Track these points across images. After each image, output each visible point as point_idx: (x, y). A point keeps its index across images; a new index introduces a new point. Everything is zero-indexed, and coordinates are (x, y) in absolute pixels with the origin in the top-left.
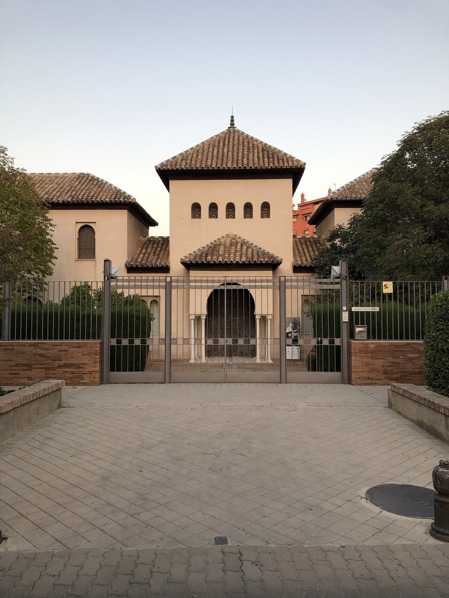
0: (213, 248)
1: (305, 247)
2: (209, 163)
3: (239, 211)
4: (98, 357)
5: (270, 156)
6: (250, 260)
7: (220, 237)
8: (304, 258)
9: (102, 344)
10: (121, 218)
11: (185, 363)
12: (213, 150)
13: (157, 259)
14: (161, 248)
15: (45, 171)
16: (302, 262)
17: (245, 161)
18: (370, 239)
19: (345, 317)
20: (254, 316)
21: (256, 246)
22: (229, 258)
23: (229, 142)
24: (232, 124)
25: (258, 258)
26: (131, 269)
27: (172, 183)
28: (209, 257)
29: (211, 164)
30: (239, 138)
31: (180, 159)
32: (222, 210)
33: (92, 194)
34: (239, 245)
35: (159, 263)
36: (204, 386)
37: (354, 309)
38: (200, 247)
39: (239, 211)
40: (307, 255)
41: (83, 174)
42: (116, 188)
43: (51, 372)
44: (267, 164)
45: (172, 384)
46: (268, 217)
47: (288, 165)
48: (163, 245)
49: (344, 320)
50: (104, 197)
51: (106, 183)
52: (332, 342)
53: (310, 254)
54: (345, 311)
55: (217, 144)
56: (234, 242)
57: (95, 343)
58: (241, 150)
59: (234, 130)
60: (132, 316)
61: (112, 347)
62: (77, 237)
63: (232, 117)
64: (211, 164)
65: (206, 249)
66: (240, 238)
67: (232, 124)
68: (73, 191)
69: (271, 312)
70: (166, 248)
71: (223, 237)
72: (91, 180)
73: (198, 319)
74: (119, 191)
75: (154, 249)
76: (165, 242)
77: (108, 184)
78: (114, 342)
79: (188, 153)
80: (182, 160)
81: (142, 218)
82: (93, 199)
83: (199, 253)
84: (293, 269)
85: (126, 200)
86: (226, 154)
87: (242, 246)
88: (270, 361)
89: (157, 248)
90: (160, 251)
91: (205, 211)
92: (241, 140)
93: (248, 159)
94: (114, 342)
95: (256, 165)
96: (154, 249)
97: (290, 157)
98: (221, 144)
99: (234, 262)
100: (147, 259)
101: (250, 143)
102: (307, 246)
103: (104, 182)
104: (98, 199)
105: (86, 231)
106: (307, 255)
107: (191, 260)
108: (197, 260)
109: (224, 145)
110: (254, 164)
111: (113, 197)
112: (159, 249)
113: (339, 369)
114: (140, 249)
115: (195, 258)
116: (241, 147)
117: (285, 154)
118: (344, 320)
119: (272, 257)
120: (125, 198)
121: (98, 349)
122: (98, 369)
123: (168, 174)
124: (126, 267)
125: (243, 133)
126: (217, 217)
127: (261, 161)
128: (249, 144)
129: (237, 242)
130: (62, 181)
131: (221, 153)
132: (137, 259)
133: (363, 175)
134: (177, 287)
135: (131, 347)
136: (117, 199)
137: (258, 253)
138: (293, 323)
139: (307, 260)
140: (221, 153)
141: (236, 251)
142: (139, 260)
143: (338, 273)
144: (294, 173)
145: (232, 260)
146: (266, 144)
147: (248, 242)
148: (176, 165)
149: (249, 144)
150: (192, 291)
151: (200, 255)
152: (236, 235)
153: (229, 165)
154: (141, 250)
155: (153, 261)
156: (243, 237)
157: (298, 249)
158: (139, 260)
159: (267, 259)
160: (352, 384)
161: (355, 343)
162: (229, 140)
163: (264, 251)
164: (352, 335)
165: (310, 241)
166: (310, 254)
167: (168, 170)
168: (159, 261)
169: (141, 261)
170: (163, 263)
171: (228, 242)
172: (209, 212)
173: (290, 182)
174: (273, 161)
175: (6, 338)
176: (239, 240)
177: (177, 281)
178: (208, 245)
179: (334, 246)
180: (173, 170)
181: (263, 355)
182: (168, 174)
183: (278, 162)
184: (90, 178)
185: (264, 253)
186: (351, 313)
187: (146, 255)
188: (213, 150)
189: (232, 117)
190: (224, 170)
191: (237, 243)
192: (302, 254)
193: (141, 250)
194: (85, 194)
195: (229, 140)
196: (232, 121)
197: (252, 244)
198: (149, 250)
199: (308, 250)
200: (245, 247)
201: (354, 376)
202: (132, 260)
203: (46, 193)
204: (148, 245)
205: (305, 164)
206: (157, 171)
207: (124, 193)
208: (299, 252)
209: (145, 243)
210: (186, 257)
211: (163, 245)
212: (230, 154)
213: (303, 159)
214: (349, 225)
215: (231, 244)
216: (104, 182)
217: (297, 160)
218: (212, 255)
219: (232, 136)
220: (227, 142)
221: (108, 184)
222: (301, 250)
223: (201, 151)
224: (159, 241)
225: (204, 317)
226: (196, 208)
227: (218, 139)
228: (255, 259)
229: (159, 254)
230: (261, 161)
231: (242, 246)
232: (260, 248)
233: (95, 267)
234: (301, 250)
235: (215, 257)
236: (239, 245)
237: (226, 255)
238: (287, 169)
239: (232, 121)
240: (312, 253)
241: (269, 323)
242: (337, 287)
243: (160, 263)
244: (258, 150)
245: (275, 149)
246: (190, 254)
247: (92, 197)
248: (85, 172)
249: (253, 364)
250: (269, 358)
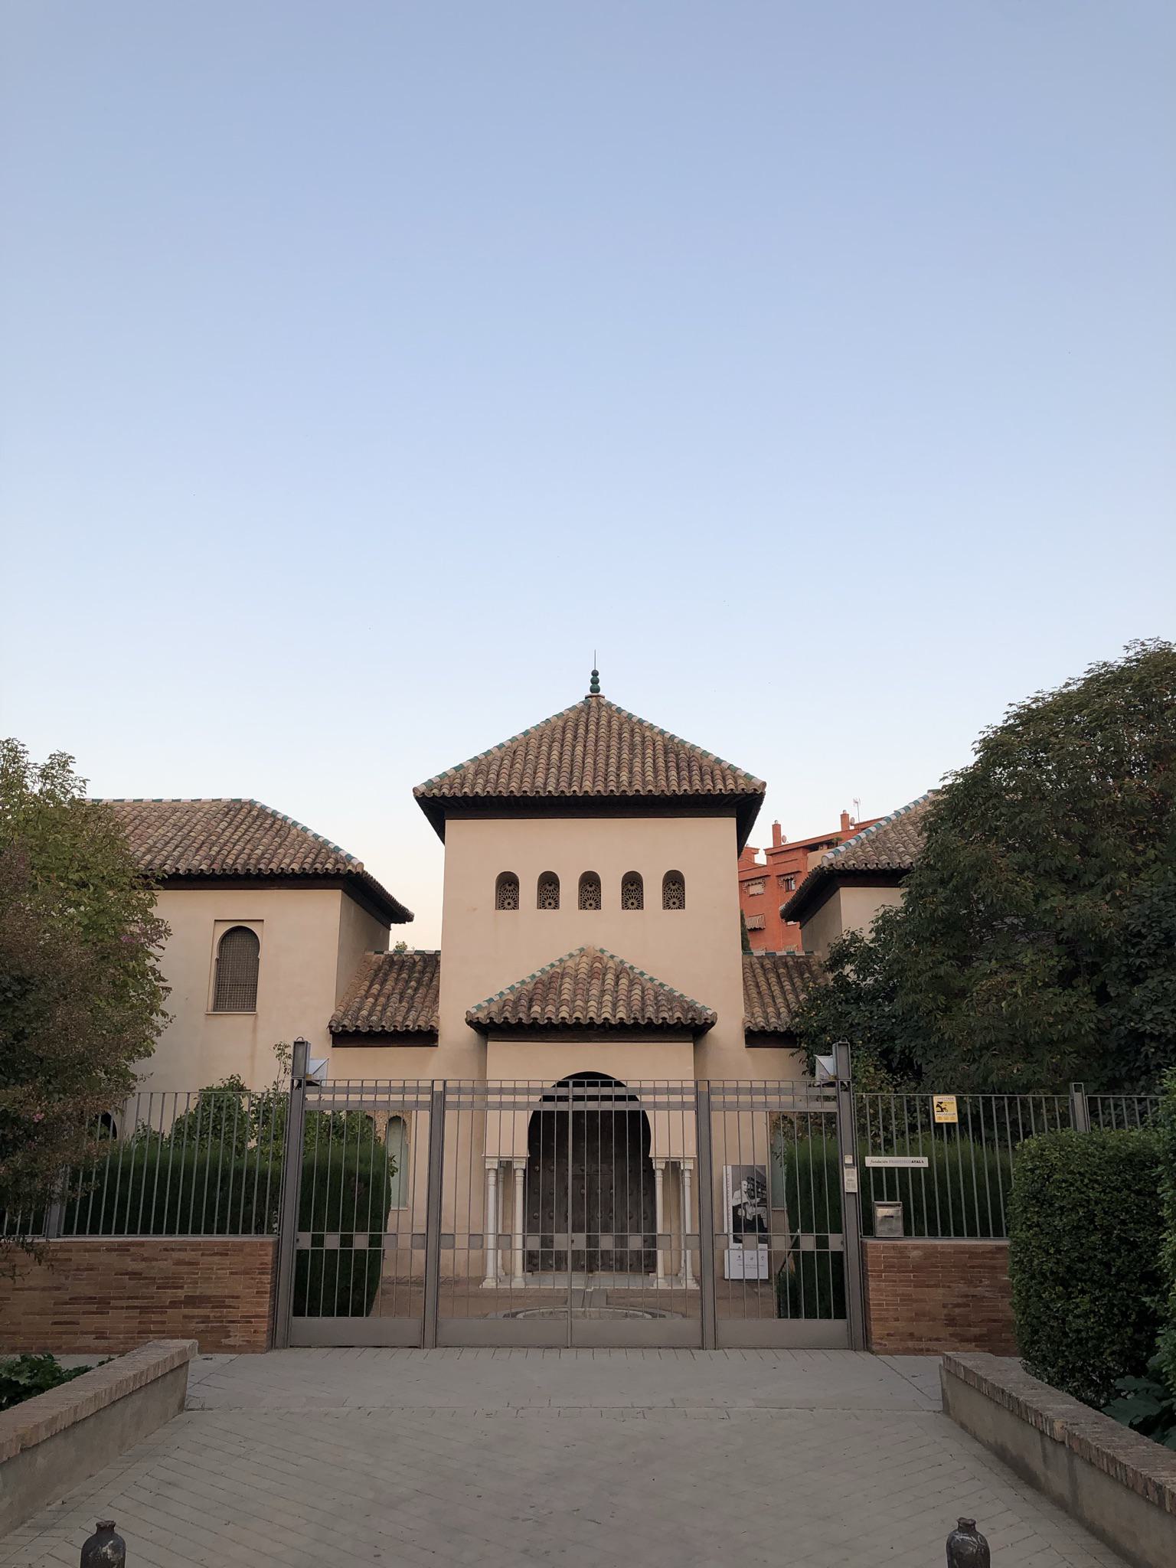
0: (547, 984)
1: (773, 980)
2: (540, 781)
3: (611, 890)
4: (267, 1278)
5: (683, 764)
6: (638, 1015)
7: (564, 955)
8: (770, 1010)
9: (278, 1246)
10: (327, 909)
11: (472, 1288)
12: (550, 747)
13: (408, 1011)
14: (419, 982)
15: (148, 795)
16: (766, 1018)
17: (624, 777)
18: (920, 973)
19: (850, 1181)
20: (649, 1162)
21: (652, 980)
22: (586, 1009)
23: (587, 731)
24: (595, 689)
25: (657, 1011)
26: (342, 1037)
27: (450, 825)
28: (536, 1008)
29: (545, 784)
30: (609, 722)
31: (472, 770)
32: (569, 890)
33: (258, 852)
34: (610, 977)
36: (518, 1355)
37: (871, 1161)
38: (514, 981)
39: (611, 890)
40: (779, 1000)
41: (239, 800)
42: (316, 837)
43: (154, 1317)
44: (674, 784)
45: (439, 1351)
47: (725, 786)
48: (423, 972)
49: (848, 1189)
50: (287, 861)
51: (295, 824)
52: (822, 1242)
53: (786, 999)
54: (849, 1166)
55: (558, 736)
56: (600, 969)
57: (262, 1244)
58: (614, 751)
59: (599, 704)
60: (350, 1174)
61: (301, 1255)
62: (216, 956)
63: (595, 674)
64: (545, 784)
65: (530, 987)
66: (612, 957)
67: (595, 689)
68: (213, 845)
69: (691, 1150)
70: (431, 980)
71: (571, 956)
72: (258, 817)
73: (506, 1168)
74: (326, 843)
75: (400, 985)
76: (430, 962)
77: (299, 827)
78: (305, 1241)
79: (490, 758)
80: (476, 774)
81: (375, 906)
82: (262, 866)
83: (511, 997)
85: (340, 866)
86: (579, 759)
87: (617, 978)
88: (692, 1285)
89: (407, 982)
90: (416, 990)
91: (528, 891)
92: (615, 726)
93: (631, 772)
94: (305, 1241)
95: (650, 787)
96: (400, 985)
97: (730, 767)
98: (569, 736)
99: (599, 1021)
100: (384, 1009)
101: (634, 734)
102: (778, 976)
103: (290, 822)
104: (272, 866)
105: (238, 940)
106: (779, 1000)
107: (493, 1015)
108: (508, 1015)
109: (575, 737)
110: (644, 783)
111: (309, 860)
112: (413, 984)
113: (841, 1314)
114: (367, 983)
115: (501, 1011)
116: (614, 743)
117: (718, 761)
118: (848, 1189)
119: (691, 1007)
120: (337, 861)
121: (269, 1259)
122: (265, 1309)
123: (442, 806)
124: (332, 1032)
125: (619, 710)
126: (556, 907)
127: (662, 777)
128: (632, 736)
129: (606, 969)
130: (188, 821)
131: (567, 757)
132: (360, 1009)
133: (907, 808)
134: (458, 1106)
135: (346, 1255)
136: (318, 866)
137: (656, 998)
138: (750, 1180)
139: (778, 1015)
140: (567, 757)
141: (603, 992)
142: (364, 1013)
143: (832, 1072)
144: (742, 804)
145: (592, 1014)
146: (673, 737)
147: (632, 968)
148: (462, 785)
149: (632, 736)
150: (492, 1115)
151: (514, 1002)
152: (602, 951)
153: (587, 785)
154: (370, 987)
155: (398, 1016)
156: (620, 957)
157: (757, 986)
158: (364, 1013)
159: (678, 1015)
160: (872, 1353)
161: (875, 1247)
162: (587, 726)
163: (671, 991)
164: (868, 1226)
165: (786, 965)
166: (786, 999)
167: (444, 797)
168: (413, 1014)
169: (369, 1016)
171: (584, 968)
172: (539, 894)
174: (690, 777)
175: (53, 1230)
176: (611, 964)
177: (459, 1091)
178: (534, 976)
179: (842, 982)
180: (454, 797)
181: (675, 1266)
182: (442, 806)
183: (702, 780)
184: (255, 813)
185: (673, 999)
186: (864, 1173)
187: (382, 1000)
188: (550, 747)
189: (595, 674)
190: (574, 797)
191: (605, 970)
192: (768, 1000)
193: (370, 987)
194: (241, 852)
195: (587, 726)
196: (595, 681)
197: (642, 974)
198: (389, 985)
199: (782, 987)
200: (624, 981)
201: (876, 1330)
202: (345, 1014)
203: (149, 851)
204: (386, 975)
205: (764, 784)
206: (417, 799)
207: (337, 849)
208: (759, 993)
209: (380, 969)
210: (479, 1008)
211: (423, 972)
212: (589, 760)
213: (759, 774)
214: (874, 935)
215: (592, 974)
216: (290, 822)
217: (747, 776)
218: (545, 1001)
219: (594, 719)
220: (581, 731)
221: (299, 827)
222: (764, 987)
223: (521, 753)
224: (415, 963)
225: (520, 1166)
226: (508, 884)
227: (561, 723)
228: (650, 1012)
229: (412, 998)
230: (662, 777)
231: (617, 978)
232: (662, 985)
233: (255, 1030)
234: (764, 987)
235: (550, 1008)
236: (610, 977)
237: (579, 1003)
238: (721, 796)
239: (595, 681)
240: (791, 997)
241: (687, 1181)
242: (830, 1107)
243: (415, 1022)
244: (654, 750)
245: (693, 748)
246: (491, 1000)
247: (258, 862)
248: (245, 796)
249: (649, 1294)
250: (689, 1276)
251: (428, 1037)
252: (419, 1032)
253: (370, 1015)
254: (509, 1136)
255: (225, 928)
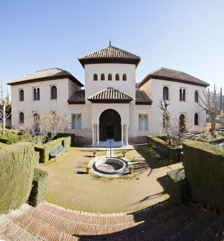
3: (114, 77)
10: (66, 81)
27: (85, 66)
35: (81, 100)
39: (114, 77)
40: (140, 97)
46: (126, 80)
76: (84, 91)
84: (136, 103)
90: (82, 95)
106: (140, 97)
123: (84, 62)
142: (73, 99)
158: (73, 99)
170: (82, 100)
173: (135, 65)
200: (117, 93)
204: (78, 94)
213: (140, 56)
225: (98, 125)
251: (83, 103)
252: (82, 102)
253: (74, 99)
254: (96, 121)
255: (52, 86)
